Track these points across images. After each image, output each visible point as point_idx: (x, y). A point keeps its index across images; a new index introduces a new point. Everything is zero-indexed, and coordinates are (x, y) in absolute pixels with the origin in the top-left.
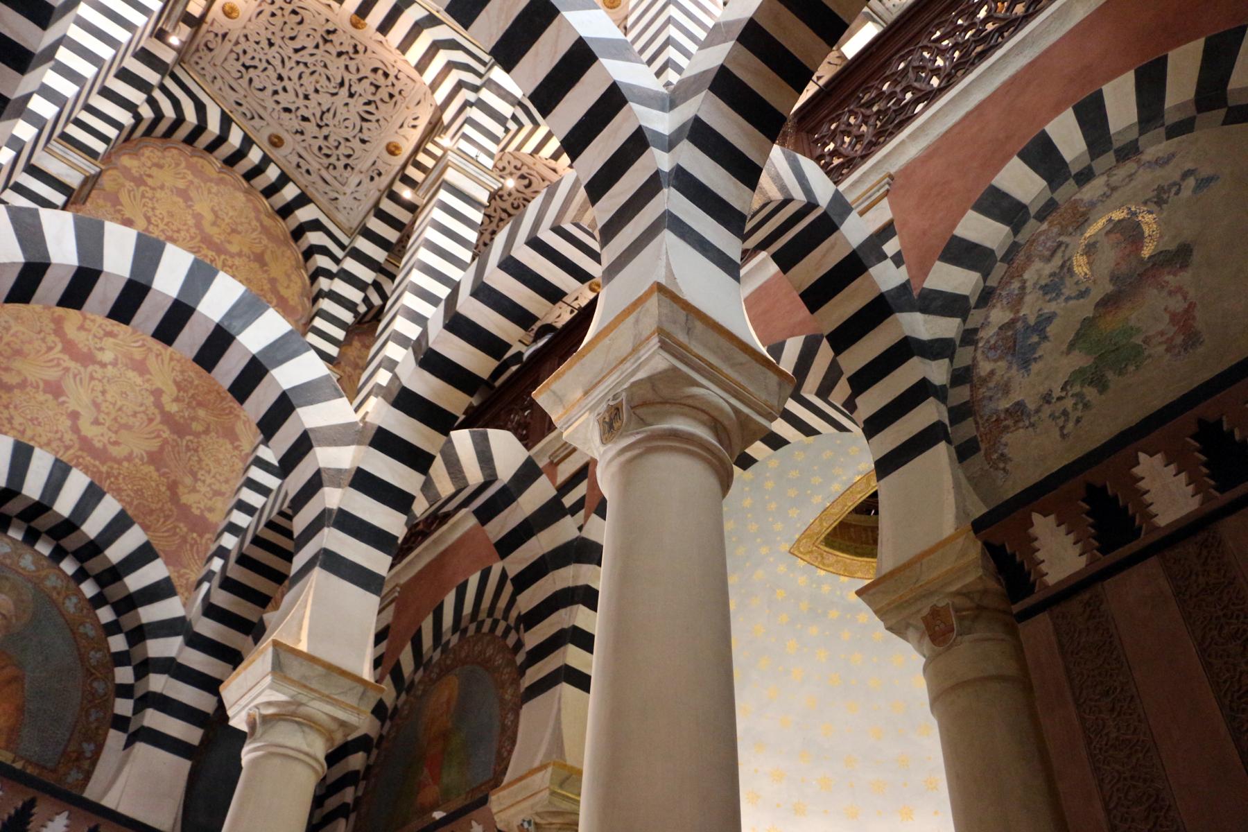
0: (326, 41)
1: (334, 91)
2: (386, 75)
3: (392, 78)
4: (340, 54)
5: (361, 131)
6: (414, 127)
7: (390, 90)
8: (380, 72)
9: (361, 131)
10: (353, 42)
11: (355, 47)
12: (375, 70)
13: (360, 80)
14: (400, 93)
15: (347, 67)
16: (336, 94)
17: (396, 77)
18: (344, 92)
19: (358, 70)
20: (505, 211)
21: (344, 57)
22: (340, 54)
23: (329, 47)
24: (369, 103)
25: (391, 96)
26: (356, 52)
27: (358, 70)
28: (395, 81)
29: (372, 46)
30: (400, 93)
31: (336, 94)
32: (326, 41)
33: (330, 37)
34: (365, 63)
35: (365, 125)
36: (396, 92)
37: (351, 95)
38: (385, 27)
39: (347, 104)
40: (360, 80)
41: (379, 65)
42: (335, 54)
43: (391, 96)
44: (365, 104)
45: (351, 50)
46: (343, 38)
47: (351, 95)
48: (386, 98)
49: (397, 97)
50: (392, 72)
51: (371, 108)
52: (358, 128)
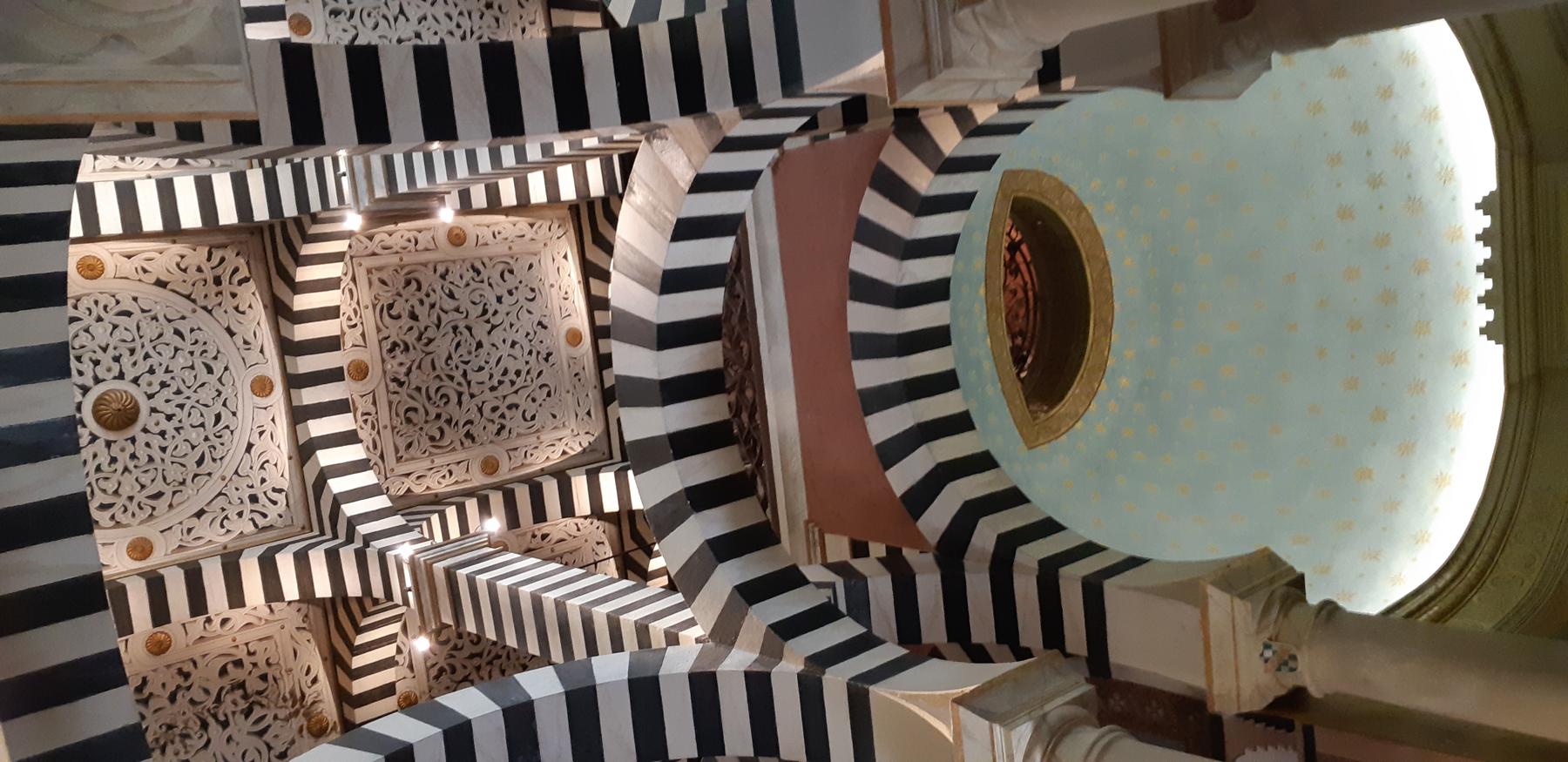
0: (145, 702)
1: (205, 738)
2: (239, 663)
3: (247, 661)
4: (172, 698)
5: (270, 748)
6: (315, 681)
7: (256, 673)
8: (230, 667)
9: (270, 748)
10: (174, 670)
11: (180, 671)
12: (223, 671)
13: (218, 700)
14: (268, 664)
15: (192, 702)
16: (209, 741)
17: (250, 654)
18: (214, 729)
19: (207, 691)
20: (472, 656)
21: (179, 696)
22: (172, 698)
23: (153, 704)
24: (247, 713)
25: (264, 677)
26: (187, 676)
27: (207, 691)
28: (253, 659)
29: (196, 653)
30: (268, 664)
31: (209, 741)
32: (145, 702)
33: (146, 692)
34: (207, 676)
35: (267, 737)
36: (263, 669)
37: (225, 724)
38: (198, 604)
39: (229, 739)
40: (218, 700)
41: (223, 661)
42: (167, 703)
43: (264, 677)
44: (247, 717)
45: (180, 680)
46: (161, 678)
47: (225, 724)
48: (261, 686)
49: (271, 672)
50: (241, 654)
51: (257, 712)
52: (264, 749)
